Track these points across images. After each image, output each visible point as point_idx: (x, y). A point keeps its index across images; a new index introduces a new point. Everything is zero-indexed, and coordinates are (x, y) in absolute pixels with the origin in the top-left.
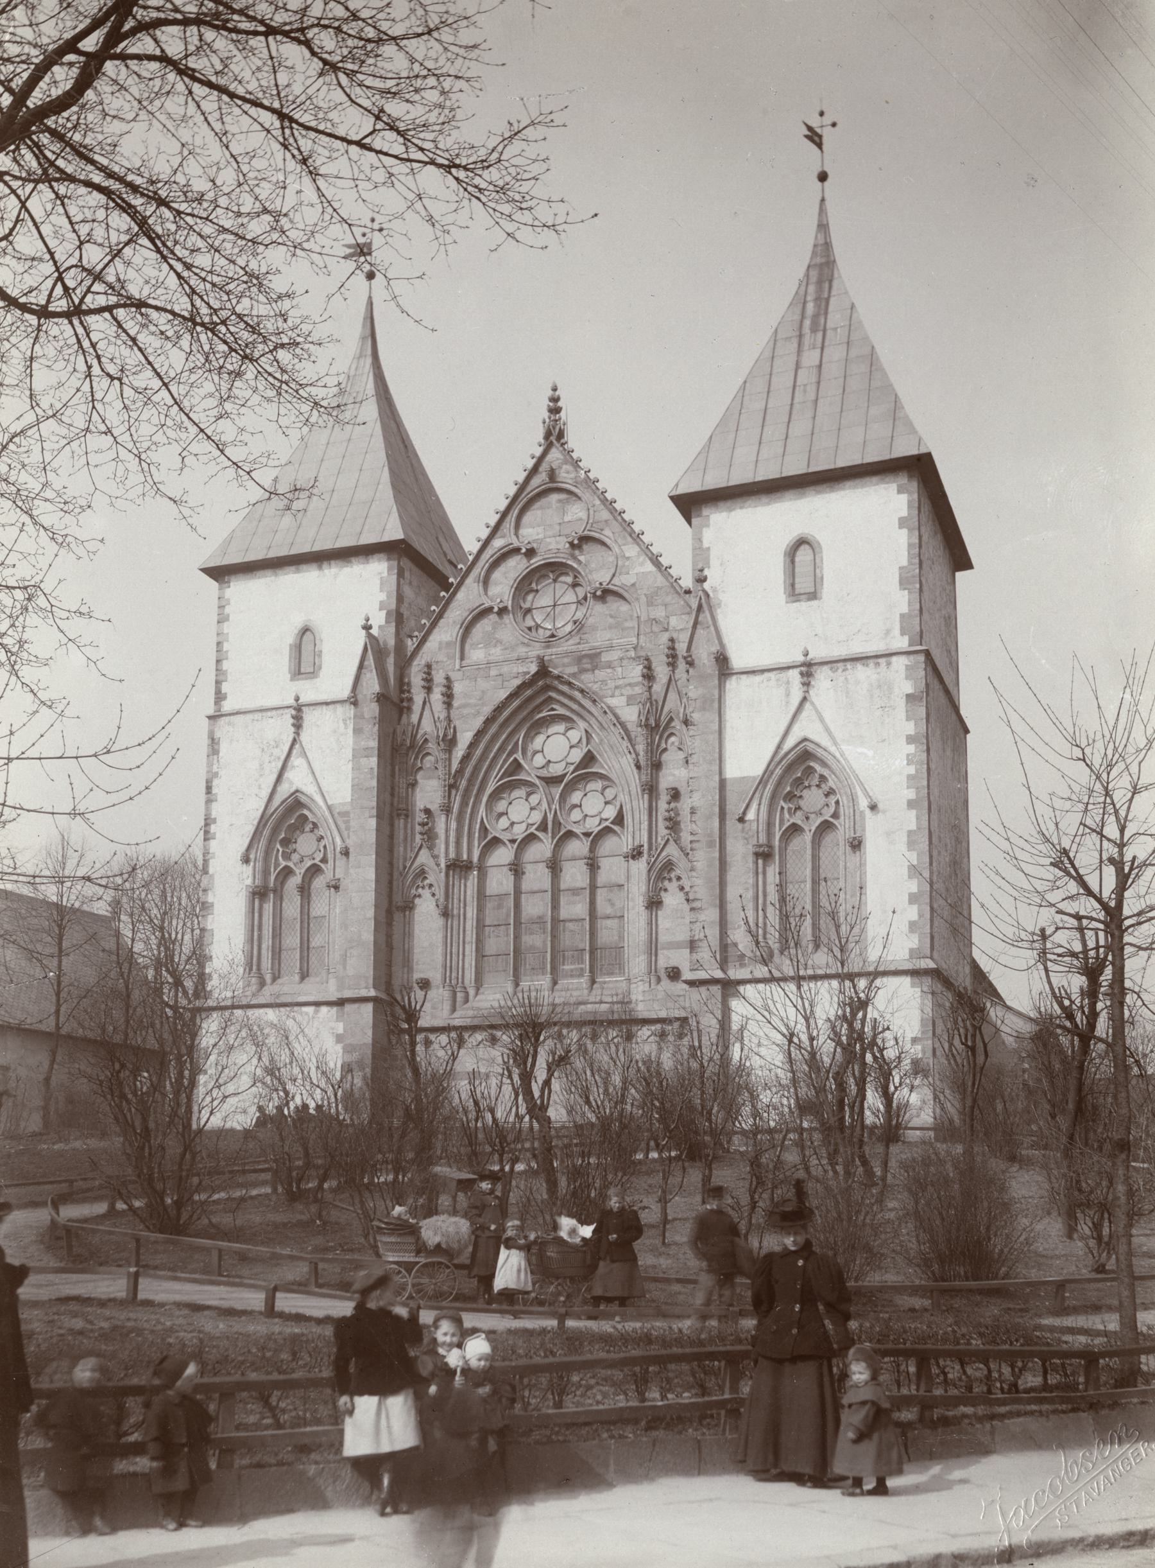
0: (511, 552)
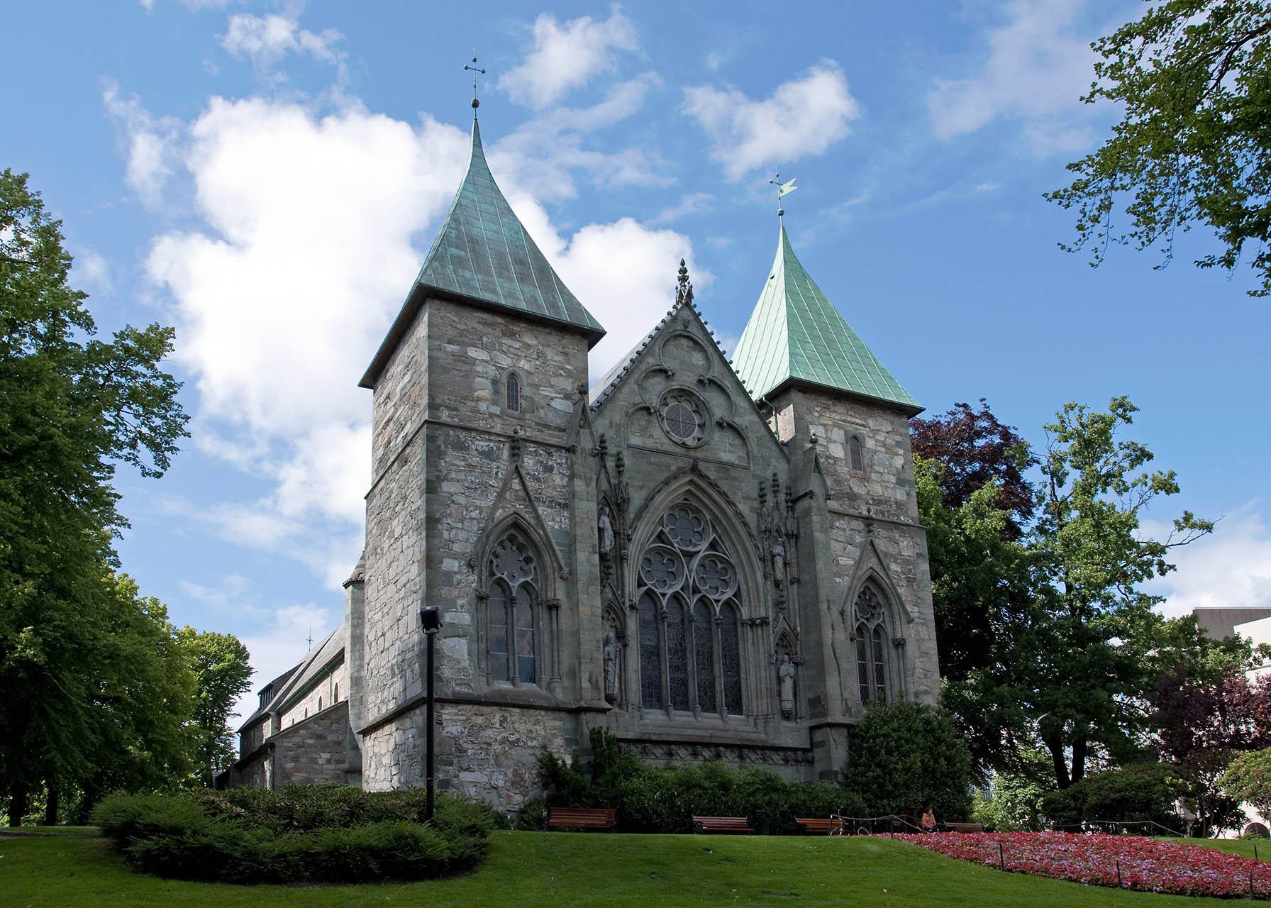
0: (663, 371)
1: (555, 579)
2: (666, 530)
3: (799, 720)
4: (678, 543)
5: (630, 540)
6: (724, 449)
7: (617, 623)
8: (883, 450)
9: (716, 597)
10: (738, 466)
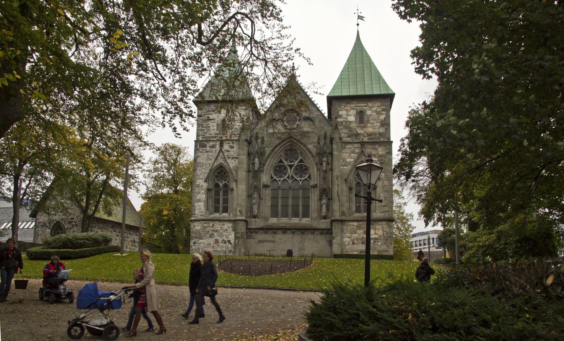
6: (306, 127)
8: (375, 114)
9: (300, 179)
10: (311, 132)
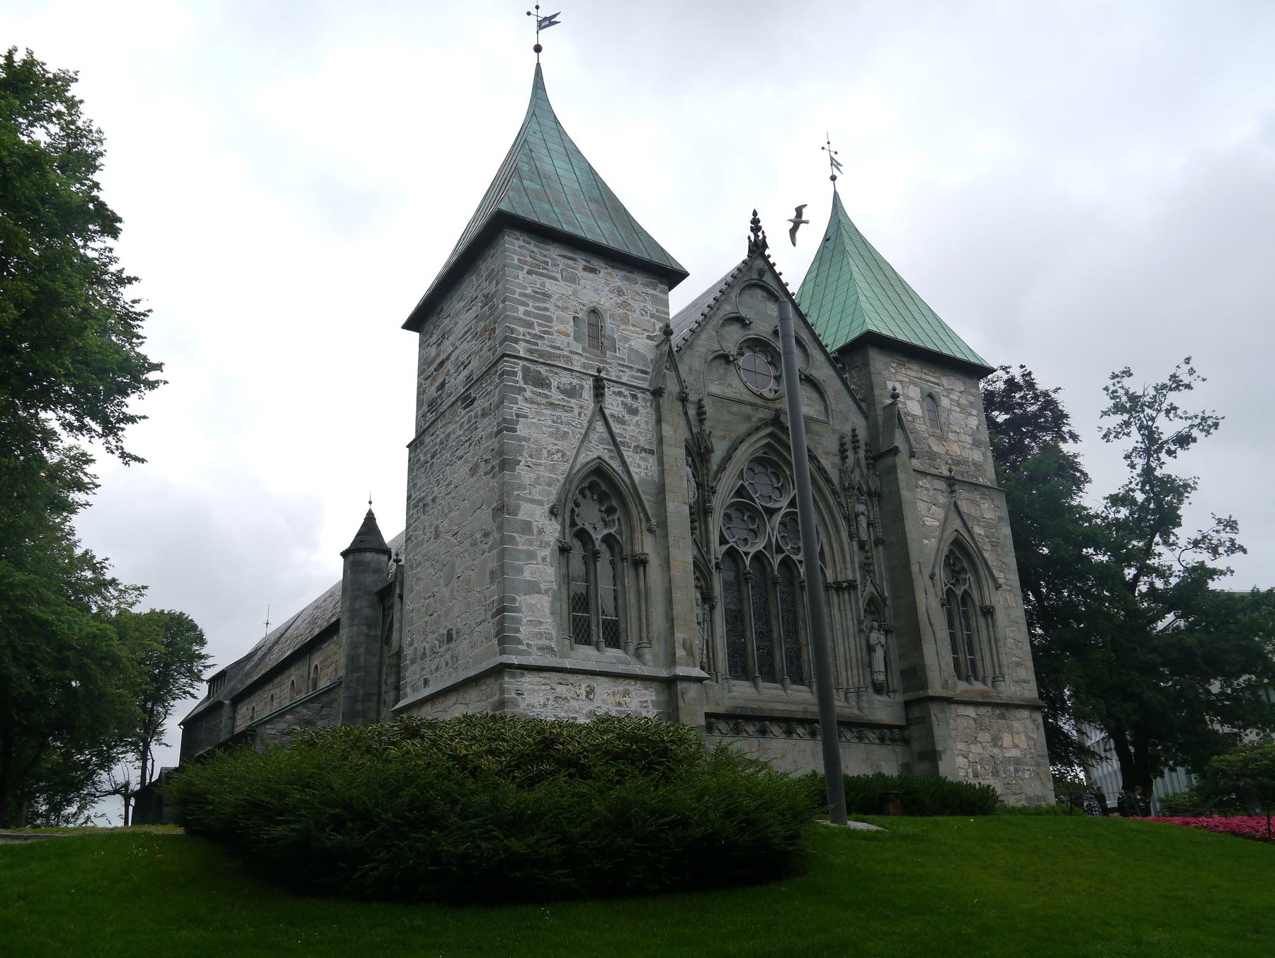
1: (642, 531)
2: (746, 484)
3: (892, 694)
4: (758, 498)
5: (714, 493)
7: (702, 583)
8: (958, 409)
